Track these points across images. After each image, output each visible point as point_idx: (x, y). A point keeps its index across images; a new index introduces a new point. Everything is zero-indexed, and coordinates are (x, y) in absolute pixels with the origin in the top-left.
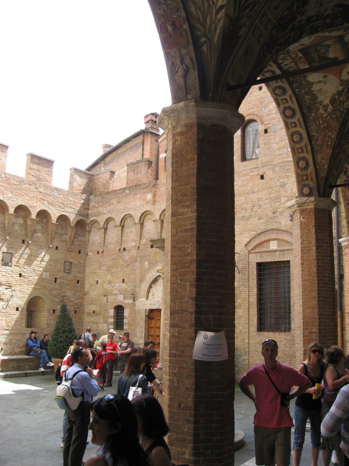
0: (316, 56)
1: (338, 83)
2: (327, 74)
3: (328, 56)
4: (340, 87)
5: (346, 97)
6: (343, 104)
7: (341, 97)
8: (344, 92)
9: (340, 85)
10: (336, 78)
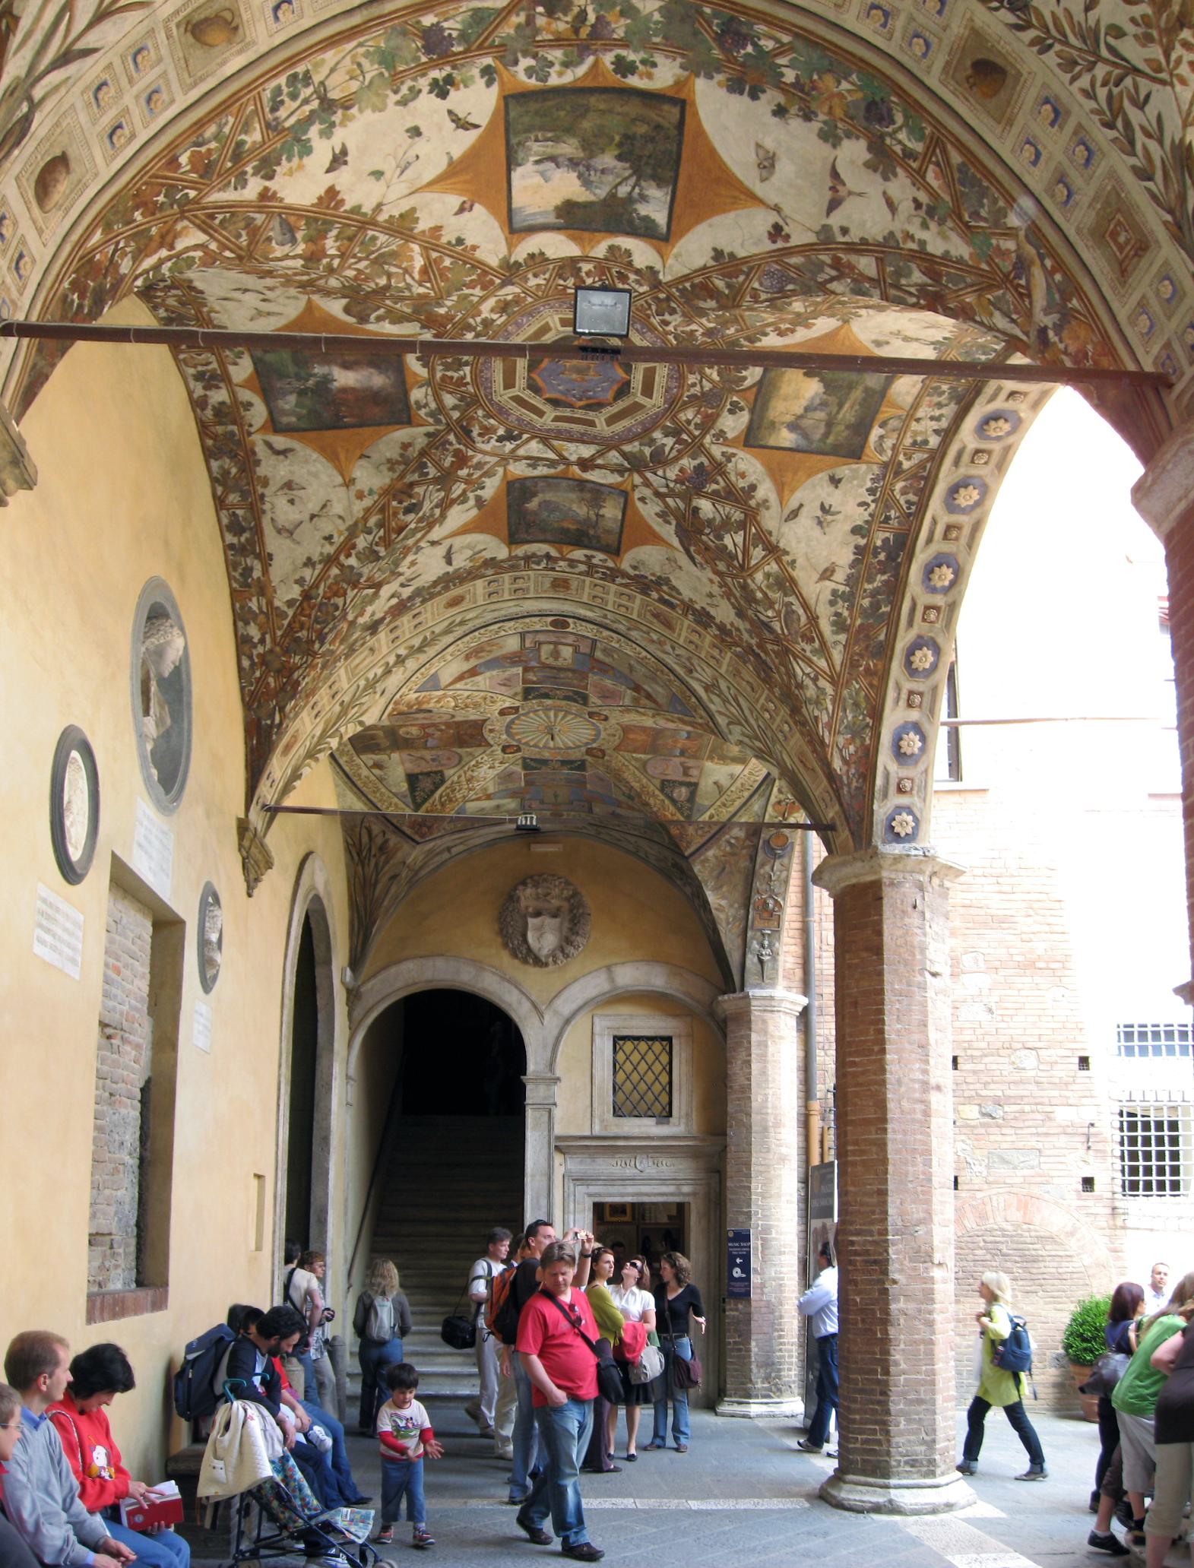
0: (847, 406)
3: (822, 390)
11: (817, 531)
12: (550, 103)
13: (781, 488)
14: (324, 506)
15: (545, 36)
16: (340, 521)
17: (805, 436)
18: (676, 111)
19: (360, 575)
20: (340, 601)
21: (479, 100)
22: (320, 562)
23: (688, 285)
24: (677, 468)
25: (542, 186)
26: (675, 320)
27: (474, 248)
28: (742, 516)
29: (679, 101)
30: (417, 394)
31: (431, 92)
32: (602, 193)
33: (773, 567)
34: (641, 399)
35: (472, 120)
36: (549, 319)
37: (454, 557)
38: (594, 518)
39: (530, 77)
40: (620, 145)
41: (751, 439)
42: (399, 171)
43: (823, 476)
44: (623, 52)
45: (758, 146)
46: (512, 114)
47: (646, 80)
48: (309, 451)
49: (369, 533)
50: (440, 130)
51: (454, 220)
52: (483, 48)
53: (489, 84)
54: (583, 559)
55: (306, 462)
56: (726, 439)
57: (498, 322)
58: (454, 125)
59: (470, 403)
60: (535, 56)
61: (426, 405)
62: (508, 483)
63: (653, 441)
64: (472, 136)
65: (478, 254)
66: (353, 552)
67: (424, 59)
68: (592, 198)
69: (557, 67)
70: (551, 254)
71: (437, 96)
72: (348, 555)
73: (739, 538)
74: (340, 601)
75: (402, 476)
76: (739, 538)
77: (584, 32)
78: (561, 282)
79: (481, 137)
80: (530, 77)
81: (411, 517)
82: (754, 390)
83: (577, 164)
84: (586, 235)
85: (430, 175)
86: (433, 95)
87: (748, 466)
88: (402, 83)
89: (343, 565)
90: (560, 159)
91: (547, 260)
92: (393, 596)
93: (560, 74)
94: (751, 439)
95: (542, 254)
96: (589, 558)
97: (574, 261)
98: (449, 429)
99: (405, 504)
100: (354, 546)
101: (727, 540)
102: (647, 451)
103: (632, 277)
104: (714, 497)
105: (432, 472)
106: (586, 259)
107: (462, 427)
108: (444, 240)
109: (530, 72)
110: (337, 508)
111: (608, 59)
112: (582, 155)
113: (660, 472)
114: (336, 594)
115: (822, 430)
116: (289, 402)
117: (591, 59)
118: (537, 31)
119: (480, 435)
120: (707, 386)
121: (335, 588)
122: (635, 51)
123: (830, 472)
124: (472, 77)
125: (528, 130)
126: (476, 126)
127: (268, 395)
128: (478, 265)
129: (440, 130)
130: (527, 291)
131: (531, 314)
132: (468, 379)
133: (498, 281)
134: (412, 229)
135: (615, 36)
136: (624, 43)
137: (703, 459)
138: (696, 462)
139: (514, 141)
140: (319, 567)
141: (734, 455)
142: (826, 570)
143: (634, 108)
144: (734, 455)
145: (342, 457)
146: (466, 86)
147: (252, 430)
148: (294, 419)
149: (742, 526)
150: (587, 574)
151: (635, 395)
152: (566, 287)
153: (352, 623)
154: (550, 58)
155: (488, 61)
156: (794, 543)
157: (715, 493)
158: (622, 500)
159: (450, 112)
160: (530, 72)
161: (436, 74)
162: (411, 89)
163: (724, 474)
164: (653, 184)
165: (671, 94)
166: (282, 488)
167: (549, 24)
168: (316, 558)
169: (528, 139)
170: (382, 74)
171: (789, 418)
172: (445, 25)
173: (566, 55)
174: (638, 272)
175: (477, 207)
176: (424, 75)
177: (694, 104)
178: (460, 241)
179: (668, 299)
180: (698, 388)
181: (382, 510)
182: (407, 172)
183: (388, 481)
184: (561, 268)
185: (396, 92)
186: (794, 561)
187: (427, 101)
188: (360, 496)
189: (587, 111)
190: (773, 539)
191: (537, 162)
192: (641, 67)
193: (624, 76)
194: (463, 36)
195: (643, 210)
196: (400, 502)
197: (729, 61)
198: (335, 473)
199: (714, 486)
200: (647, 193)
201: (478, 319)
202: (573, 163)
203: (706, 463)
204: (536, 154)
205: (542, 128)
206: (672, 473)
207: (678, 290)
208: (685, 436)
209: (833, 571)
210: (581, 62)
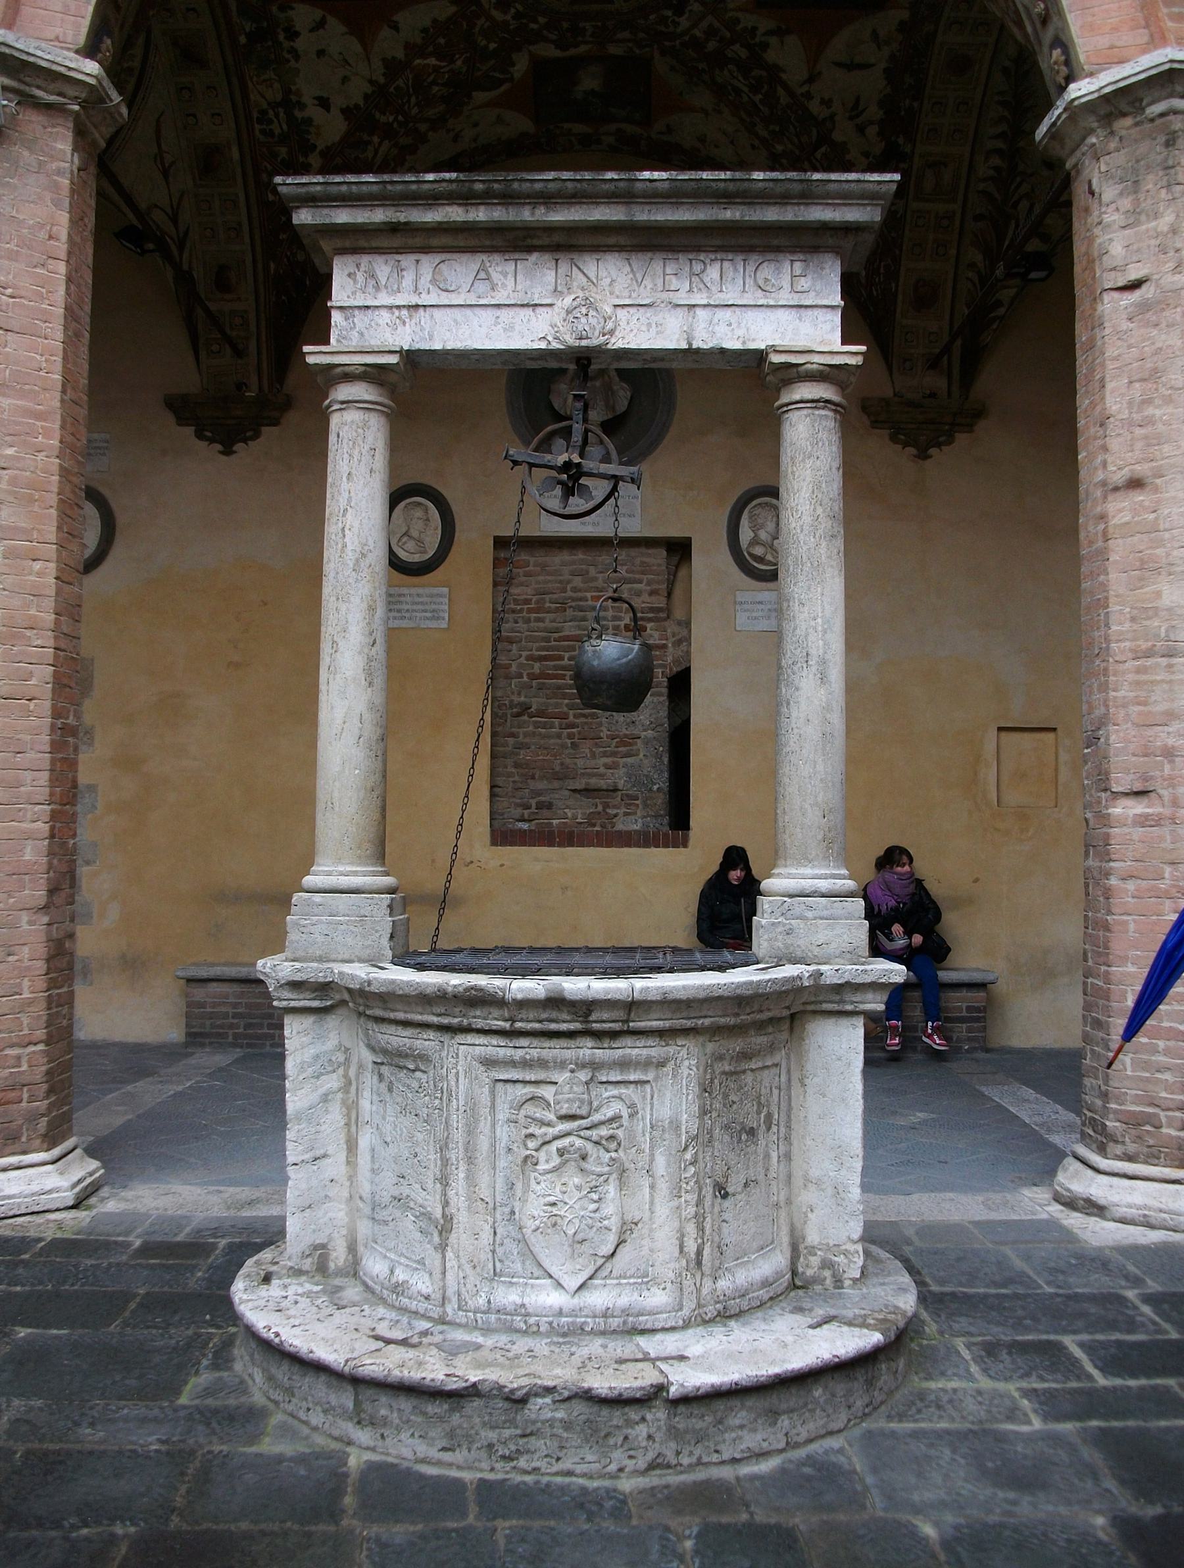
27: (435, 21)
30: (614, 50)
67: (270, 43)
85: (358, 48)
108: (419, 41)
159: (311, 31)
161: (281, 37)
162: (289, 52)
172: (248, 30)
175: (395, 18)
178: (424, 30)
182: (350, 61)
185: (288, 61)
187: (300, 44)
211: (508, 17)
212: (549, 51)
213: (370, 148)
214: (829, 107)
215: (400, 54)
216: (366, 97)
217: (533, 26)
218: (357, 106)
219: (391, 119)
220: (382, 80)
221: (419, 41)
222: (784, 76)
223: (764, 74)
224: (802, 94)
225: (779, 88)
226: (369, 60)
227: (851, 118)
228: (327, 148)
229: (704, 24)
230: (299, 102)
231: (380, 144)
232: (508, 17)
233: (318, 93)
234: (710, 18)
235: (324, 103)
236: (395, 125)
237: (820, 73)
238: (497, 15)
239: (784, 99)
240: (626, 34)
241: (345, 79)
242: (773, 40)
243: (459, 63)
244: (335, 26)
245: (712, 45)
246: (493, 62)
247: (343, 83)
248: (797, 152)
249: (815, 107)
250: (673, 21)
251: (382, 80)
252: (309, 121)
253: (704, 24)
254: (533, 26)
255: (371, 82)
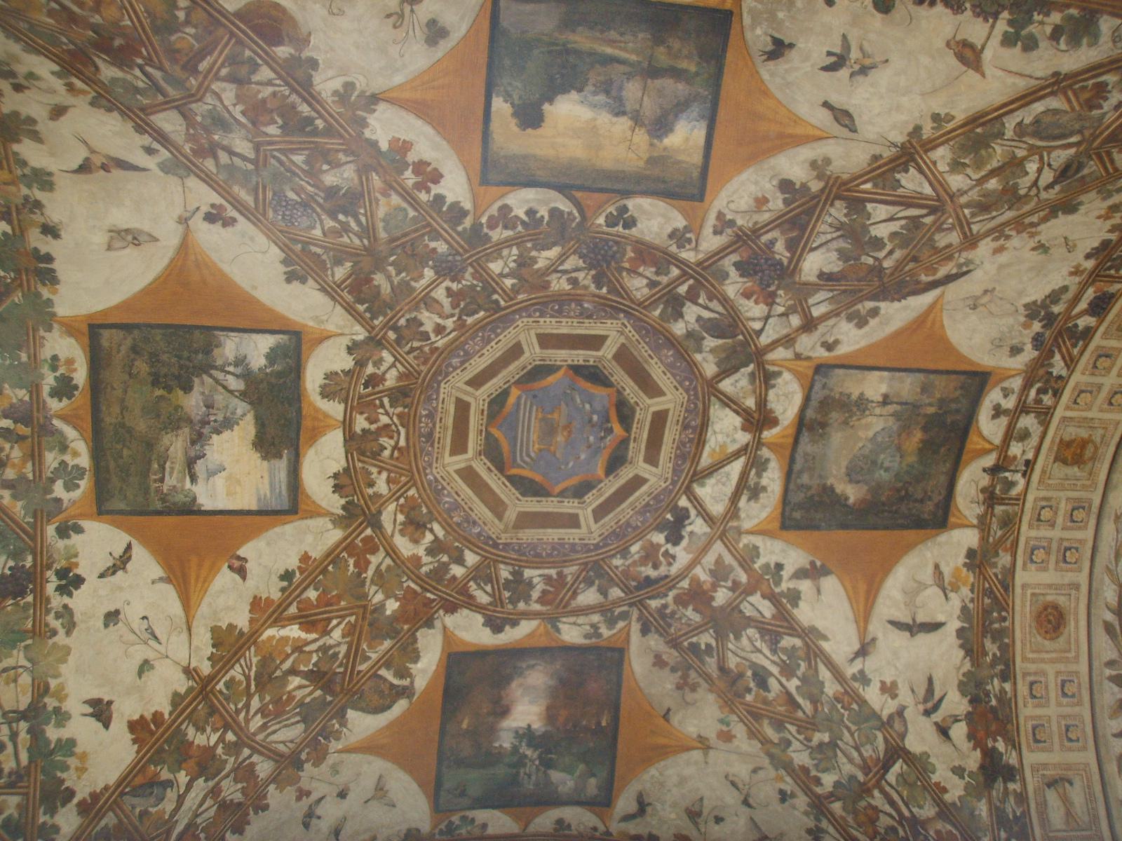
1: (361, 83)
2: (445, 46)
3: (574, 95)
4: (337, 84)
5: (264, 101)
6: (232, 79)
7: (272, 75)
8: (294, 97)
9: (349, 86)
10: (398, 79)
11: (882, 77)
12: (112, 465)
13: (788, 140)
14: (733, 784)
15: (28, 470)
16: (761, 774)
17: (681, 107)
18: (106, 334)
19: (852, 778)
20: (884, 821)
21: (97, 541)
22: (819, 820)
23: (361, 308)
24: (743, 301)
25: (232, 472)
26: (429, 320)
27: (305, 558)
28: (838, 203)
29: (93, 332)
30: (571, 633)
31: (70, 595)
32: (241, 407)
33: (942, 156)
34: (608, 351)
35: (119, 551)
36: (451, 469)
37: (921, 618)
38: (891, 408)
39: (78, 486)
40: (169, 389)
41: (689, 190)
42: (152, 643)
43: (767, 71)
44: (46, 390)
45: (109, 248)
46: (122, 506)
47: (76, 365)
48: (646, 777)
49: (789, 743)
50: (120, 589)
51: (250, 582)
52: (34, 534)
53: (79, 530)
54: (1004, 421)
55: (662, 785)
56: (687, 229)
57: (440, 533)
58: (120, 573)
59: (595, 572)
60: (53, 481)
61: (593, 626)
62: (784, 526)
63: (689, 334)
64: (139, 552)
65: (316, 554)
66: (813, 773)
67: (30, 598)
68: (250, 418)
69: (67, 458)
70: (337, 462)
71: (77, 588)
72: (818, 781)
73: (879, 211)
74: (884, 821)
75: (707, 677)
76: (879, 211)
77: (23, 430)
78: (387, 453)
79: (140, 542)
80: (78, 486)
81: (772, 682)
82: (578, 195)
83: (200, 435)
84: (307, 423)
85: (174, 606)
86: (75, 593)
87: (743, 194)
88: (47, 625)
89: (831, 794)
90: (193, 454)
91: (347, 470)
92: (943, 731)
93: (76, 454)
94: (689, 190)
95: (336, 476)
96: (998, 412)
97: (350, 438)
98: (641, 604)
99: (752, 685)
100: (805, 770)
101: (882, 231)
102: (710, 342)
103: (370, 369)
104: (797, 247)
105: (706, 639)
106: (347, 424)
107: (638, 588)
108: (276, 596)
109: (70, 486)
110: (741, 770)
111: (54, 405)
112: (187, 430)
113: (757, 326)
114: (873, 821)
115: (667, 83)
116: (564, 781)
117: (56, 422)
118: (22, 477)
119: (656, 567)
120: (572, 262)
121: (862, 818)
122: (42, 377)
123: (759, 60)
124: (66, 547)
125: (147, 491)
126: (129, 547)
127: (548, 799)
128: (333, 556)
129: (120, 589)
130: (394, 496)
131: (439, 492)
132: (553, 572)
133: (369, 532)
134: (241, 633)
135: (27, 398)
136: (35, 389)
137: (728, 263)
138: (733, 272)
139: (159, 506)
140: (824, 824)
141: (720, 216)
142: (961, 58)
143: (115, 376)
144: (720, 216)
145: (662, 741)
146: (76, 556)
147: (602, 828)
148: (593, 781)
149: (857, 205)
150: (1045, 416)
151: (600, 359)
152: (395, 447)
153: (945, 811)
154: (55, 464)
155: (51, 530)
156: (904, 118)
157: (791, 245)
158: (841, 372)
159: (102, 576)
160: (70, 486)
162: (58, 616)
163: (756, 231)
164: (216, 352)
165: (86, 340)
166: (696, 824)
167: (14, 466)
168: (811, 823)
169: (158, 490)
170: (26, 647)
171: (641, 137)
173: (51, 450)
174: (360, 364)
175: (241, 552)
176: (48, 600)
177: (90, 316)
178: (287, 576)
179: (395, 328)
180: (581, 275)
181: (757, 716)
183: (711, 697)
184: (362, 453)
185: (54, 633)
186: (936, 118)
187: (80, 601)
188: (727, 737)
189: (123, 425)
190: (887, 153)
191: (194, 479)
192: (62, 370)
193: (76, 387)
194: (15, 555)
195: (258, 361)
196: (749, 690)
197: (21, 285)
198: (685, 756)
199: (780, 247)
200: (231, 358)
201: (426, 559)
202: (199, 438)
203: (735, 258)
204: (182, 480)
205: (145, 474)
206: (753, 310)
207: (374, 317)
208: (682, 290)
209: (965, 44)
210: (61, 433)
211: (421, 551)
212: (471, 629)
213: (171, 795)
214: (894, 696)
215: (242, 620)
216: (176, 699)
217: (457, 571)
218: (157, 716)
219: (214, 738)
220: (206, 669)
221: (276, 596)
222: (825, 645)
223: (798, 642)
224: (854, 678)
225: (822, 668)
226: (189, 629)
227: (927, 713)
228: (95, 796)
229: (709, 559)
230: (57, 711)
231: (189, 786)
232: (421, 551)
233: (95, 694)
234: (718, 547)
235: (101, 711)
236: (219, 750)
237: (874, 640)
238: (404, 546)
239: (831, 688)
240: (589, 597)
241: (145, 667)
242: (805, 586)
243: (337, 634)
244: (145, 564)
245: (721, 597)
246: (387, 644)
247: (140, 673)
248: (861, 777)
249: (872, 695)
250: (666, 553)
251: (206, 669)
252: (68, 746)
253: (709, 559)
254: (457, 571)
255: (188, 672)
